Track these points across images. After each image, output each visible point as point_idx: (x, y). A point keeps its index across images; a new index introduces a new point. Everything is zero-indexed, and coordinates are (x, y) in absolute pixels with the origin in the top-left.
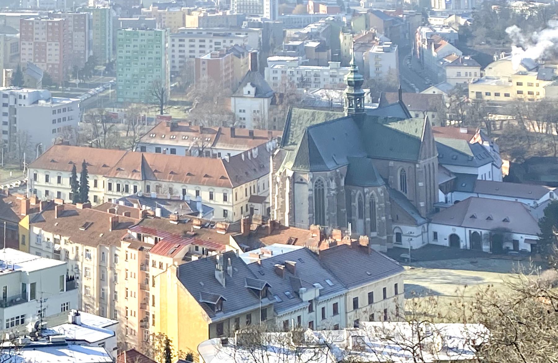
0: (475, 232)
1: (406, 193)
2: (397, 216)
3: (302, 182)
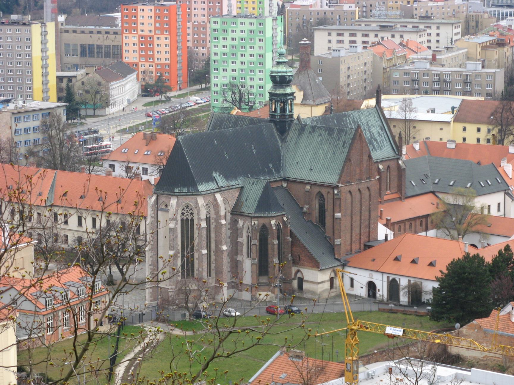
0: (394, 280)
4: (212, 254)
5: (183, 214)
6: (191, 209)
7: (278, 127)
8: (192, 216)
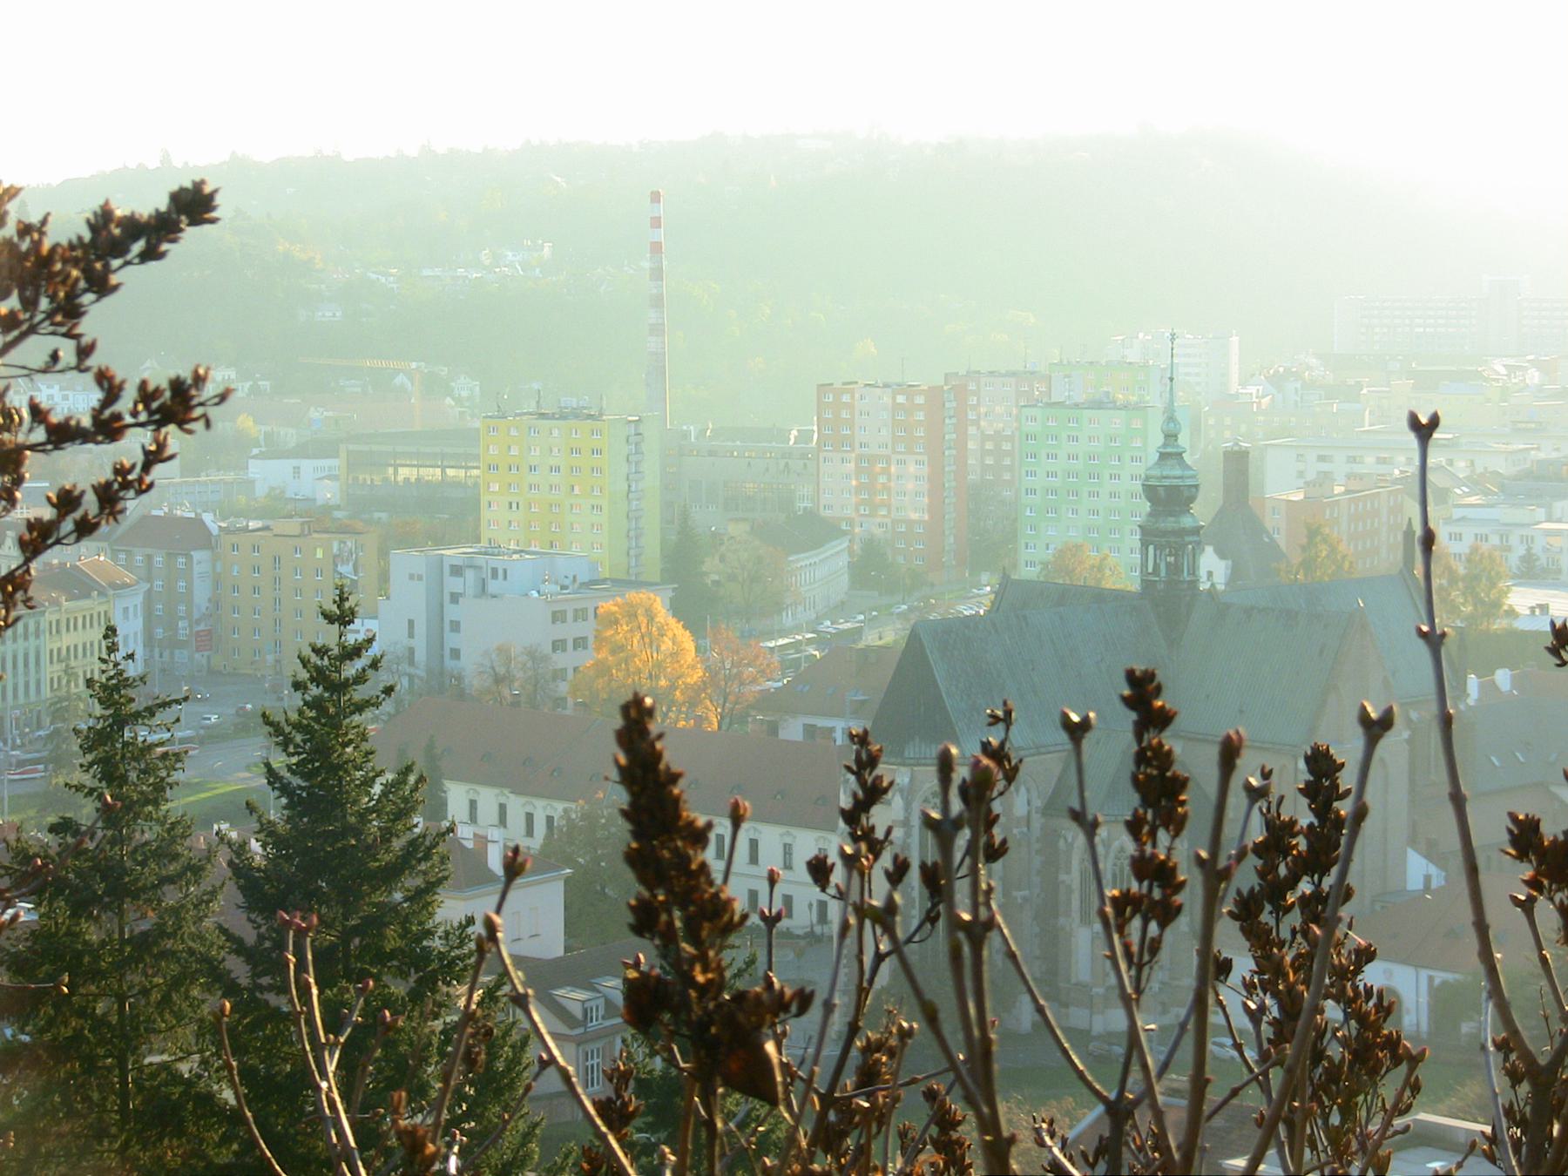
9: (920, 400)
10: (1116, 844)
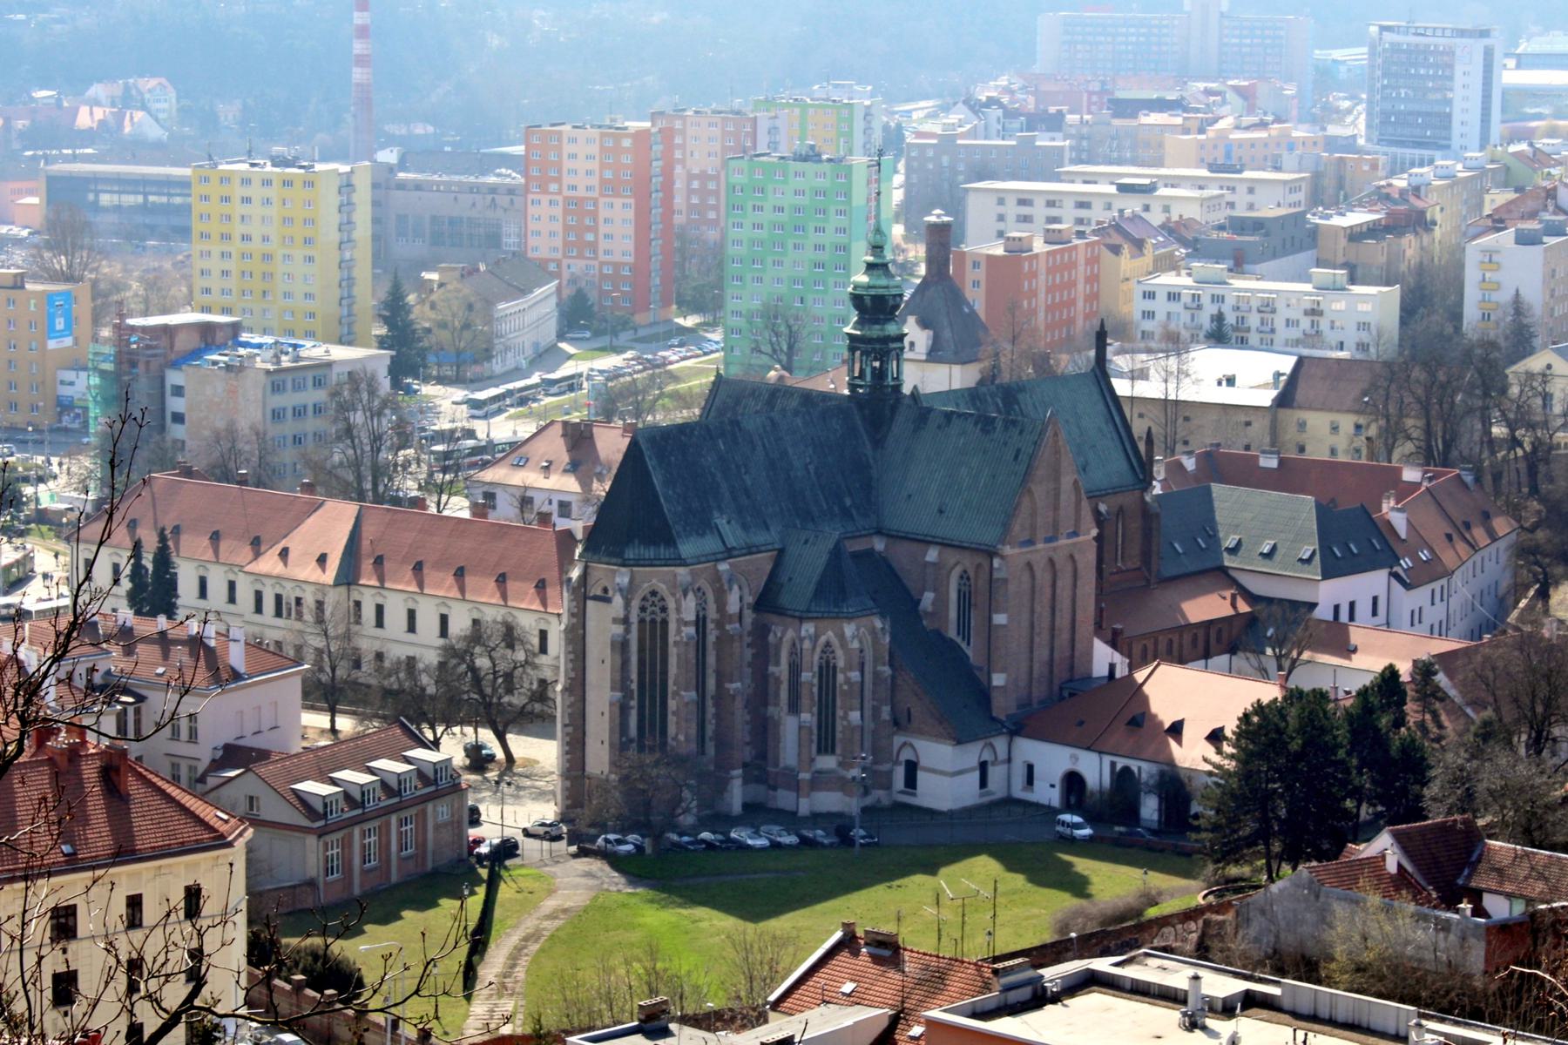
0: (1126, 770)
1: (968, 644)
2: (909, 710)
3: (605, 599)
4: (709, 702)
5: (643, 609)
6: (663, 599)
7: (867, 412)
8: (663, 615)
9: (627, 143)
10: (823, 639)
